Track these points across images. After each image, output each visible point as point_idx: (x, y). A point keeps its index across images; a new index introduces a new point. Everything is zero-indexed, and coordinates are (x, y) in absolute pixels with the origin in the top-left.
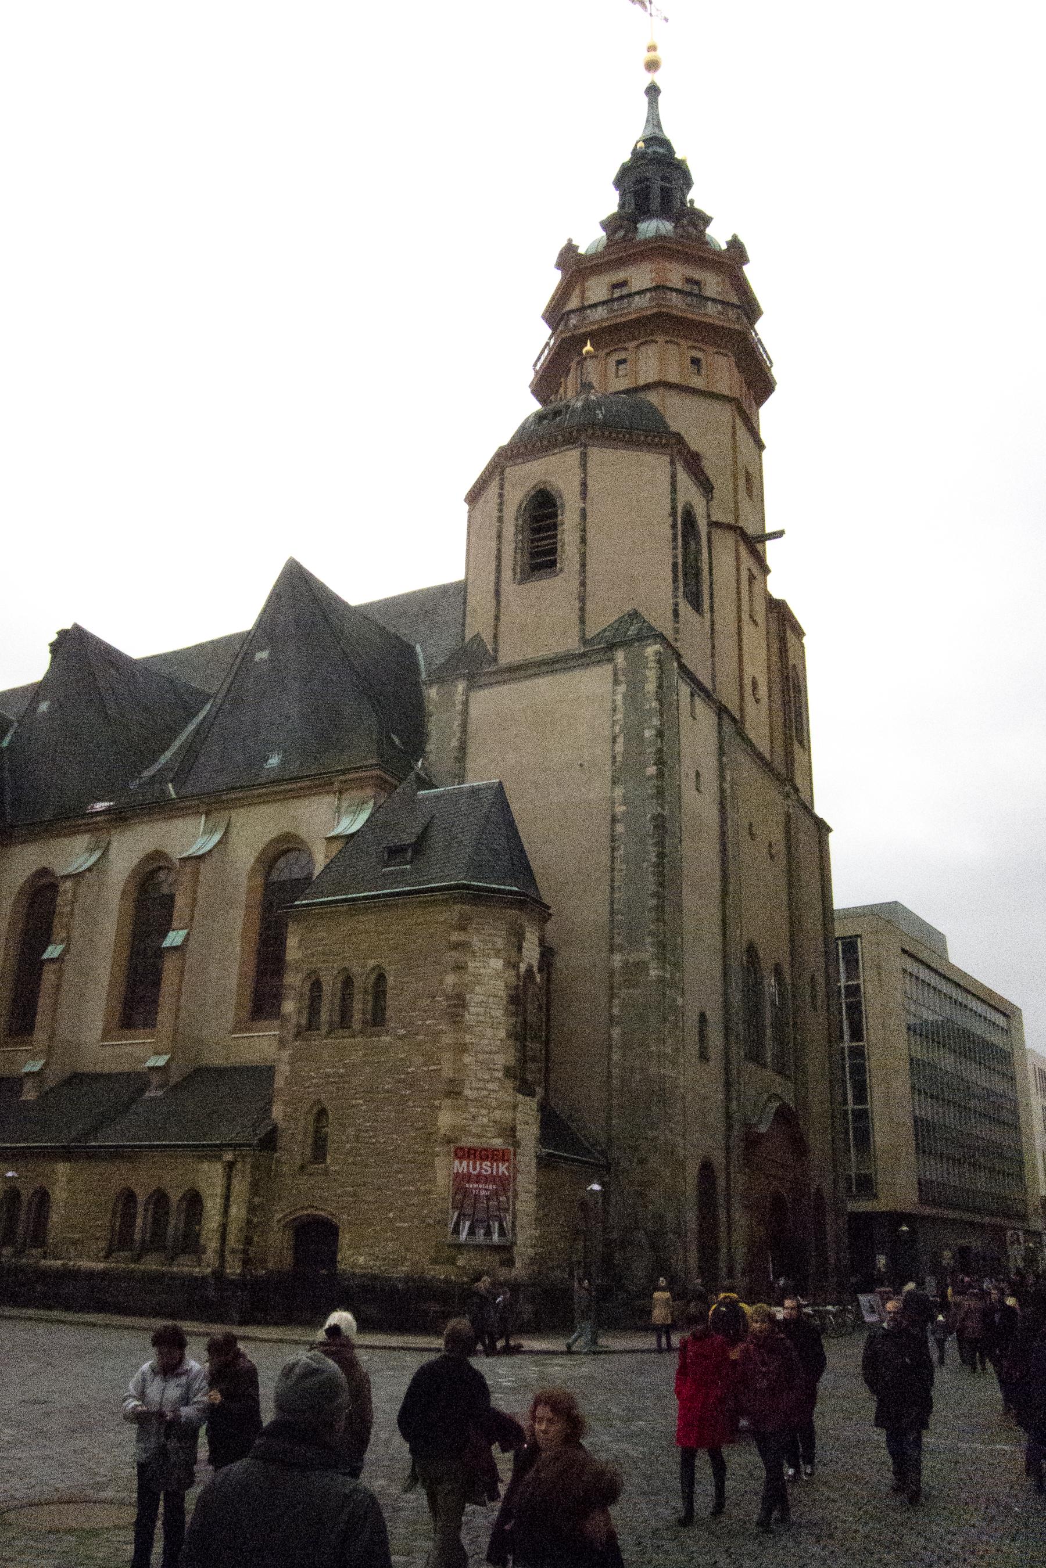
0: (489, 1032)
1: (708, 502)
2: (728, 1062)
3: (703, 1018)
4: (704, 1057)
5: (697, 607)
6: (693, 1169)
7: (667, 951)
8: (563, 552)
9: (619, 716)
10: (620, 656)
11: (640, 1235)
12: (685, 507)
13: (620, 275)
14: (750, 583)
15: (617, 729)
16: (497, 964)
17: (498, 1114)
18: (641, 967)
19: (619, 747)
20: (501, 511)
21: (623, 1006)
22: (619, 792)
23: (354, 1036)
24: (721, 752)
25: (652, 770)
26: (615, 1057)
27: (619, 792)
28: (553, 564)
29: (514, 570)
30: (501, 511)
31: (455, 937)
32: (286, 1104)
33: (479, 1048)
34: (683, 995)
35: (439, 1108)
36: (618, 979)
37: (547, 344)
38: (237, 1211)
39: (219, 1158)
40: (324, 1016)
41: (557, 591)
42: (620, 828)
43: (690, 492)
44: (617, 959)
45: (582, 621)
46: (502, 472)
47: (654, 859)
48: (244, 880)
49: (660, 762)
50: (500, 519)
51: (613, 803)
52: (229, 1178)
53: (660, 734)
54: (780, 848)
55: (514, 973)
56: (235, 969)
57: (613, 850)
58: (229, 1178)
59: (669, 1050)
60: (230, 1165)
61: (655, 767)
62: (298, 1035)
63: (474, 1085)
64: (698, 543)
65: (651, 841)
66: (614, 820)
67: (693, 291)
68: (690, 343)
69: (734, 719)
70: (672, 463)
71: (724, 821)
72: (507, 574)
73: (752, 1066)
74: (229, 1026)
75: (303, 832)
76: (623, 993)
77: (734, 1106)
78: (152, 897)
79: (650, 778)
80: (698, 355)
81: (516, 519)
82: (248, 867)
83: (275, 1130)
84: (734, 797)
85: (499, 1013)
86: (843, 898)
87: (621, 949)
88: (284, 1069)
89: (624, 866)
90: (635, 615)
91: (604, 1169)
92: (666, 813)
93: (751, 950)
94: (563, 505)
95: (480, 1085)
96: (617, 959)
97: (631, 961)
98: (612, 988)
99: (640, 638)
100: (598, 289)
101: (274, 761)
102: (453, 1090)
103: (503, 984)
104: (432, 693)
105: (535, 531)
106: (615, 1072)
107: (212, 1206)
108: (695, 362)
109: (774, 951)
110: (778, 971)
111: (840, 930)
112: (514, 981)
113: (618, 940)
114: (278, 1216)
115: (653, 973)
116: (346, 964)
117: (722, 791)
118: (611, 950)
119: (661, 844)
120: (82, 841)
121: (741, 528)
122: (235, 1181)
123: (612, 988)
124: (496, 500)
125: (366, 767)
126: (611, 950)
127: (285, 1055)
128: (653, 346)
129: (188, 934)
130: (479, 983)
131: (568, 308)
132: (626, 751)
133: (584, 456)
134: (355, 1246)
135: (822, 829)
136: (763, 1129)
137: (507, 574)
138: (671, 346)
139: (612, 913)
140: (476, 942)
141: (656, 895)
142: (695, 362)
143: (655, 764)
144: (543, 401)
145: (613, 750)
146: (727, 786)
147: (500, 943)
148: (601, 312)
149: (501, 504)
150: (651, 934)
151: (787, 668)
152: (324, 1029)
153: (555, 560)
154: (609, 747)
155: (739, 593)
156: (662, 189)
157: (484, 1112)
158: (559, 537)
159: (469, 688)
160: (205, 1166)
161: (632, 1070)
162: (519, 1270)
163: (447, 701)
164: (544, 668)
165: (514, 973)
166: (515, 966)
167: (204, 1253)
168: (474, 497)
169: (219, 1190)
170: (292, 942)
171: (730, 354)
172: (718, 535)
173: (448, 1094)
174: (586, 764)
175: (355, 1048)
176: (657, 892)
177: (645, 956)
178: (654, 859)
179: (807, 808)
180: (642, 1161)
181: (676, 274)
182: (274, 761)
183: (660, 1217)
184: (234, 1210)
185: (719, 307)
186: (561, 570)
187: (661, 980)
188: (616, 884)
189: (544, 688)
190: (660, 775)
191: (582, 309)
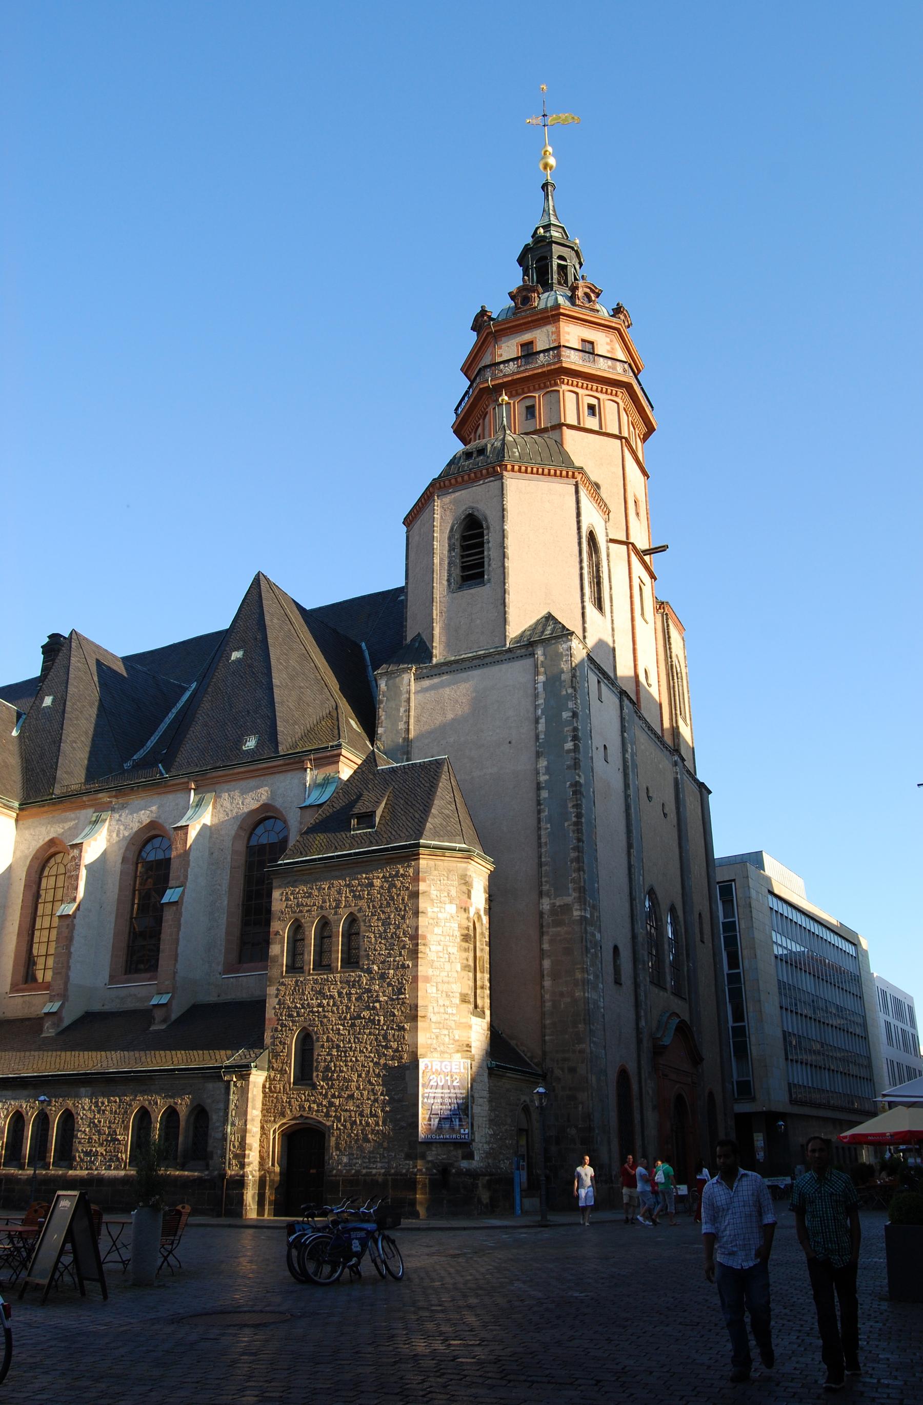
0: (447, 966)
2: (636, 985)
3: (616, 949)
4: (618, 982)
5: (600, 607)
6: (613, 1075)
7: (586, 894)
8: (489, 565)
9: (541, 701)
10: (539, 652)
11: (573, 1131)
13: (526, 337)
15: (539, 712)
16: (452, 909)
17: (457, 1034)
18: (567, 908)
19: (542, 727)
21: (551, 942)
22: (543, 763)
24: (623, 729)
25: (569, 745)
26: (547, 983)
27: (543, 763)
28: (482, 575)
29: (448, 580)
33: (439, 980)
34: (600, 932)
36: (547, 919)
37: (467, 393)
42: (544, 794)
43: (592, 517)
47: (574, 819)
49: (575, 738)
53: (575, 715)
54: (671, 808)
55: (465, 915)
56: (223, 920)
57: (539, 812)
59: (591, 977)
61: (572, 743)
63: (436, 1010)
64: (598, 557)
65: (570, 805)
66: (539, 787)
69: (630, 700)
70: (577, 492)
71: (626, 786)
73: (656, 990)
74: (220, 968)
76: (552, 930)
77: (643, 1023)
79: (569, 751)
84: (635, 766)
85: (453, 950)
86: (721, 850)
87: (549, 896)
89: (549, 826)
90: (549, 617)
91: (543, 1077)
92: (582, 781)
93: (651, 893)
94: (488, 528)
97: (558, 904)
98: (542, 926)
100: (508, 349)
101: (251, 743)
103: (457, 925)
104: (383, 685)
105: (464, 548)
106: (547, 997)
109: (669, 892)
110: (673, 909)
111: (721, 875)
112: (465, 923)
113: (545, 888)
115: (576, 913)
116: (324, 913)
117: (625, 761)
119: (577, 806)
121: (633, 544)
123: (542, 926)
126: (541, 894)
130: (437, 924)
131: (482, 364)
135: (704, 790)
136: (667, 1041)
139: (540, 865)
140: (434, 893)
141: (577, 849)
142: (591, 408)
143: (572, 740)
144: (465, 441)
145: (536, 728)
146: (628, 756)
147: (453, 893)
148: (512, 366)
153: (483, 572)
154: (533, 727)
155: (631, 597)
156: (559, 265)
157: (446, 1032)
158: (486, 553)
160: (210, 1085)
161: (562, 994)
162: (477, 1163)
164: (476, 662)
165: (465, 915)
166: (466, 910)
167: (212, 1158)
168: (409, 521)
170: (276, 894)
174: (513, 742)
176: (578, 847)
177: (568, 900)
178: (574, 819)
179: (692, 775)
180: (572, 1070)
182: (251, 743)
186: (489, 580)
187: (583, 918)
188: (543, 840)
190: (576, 749)
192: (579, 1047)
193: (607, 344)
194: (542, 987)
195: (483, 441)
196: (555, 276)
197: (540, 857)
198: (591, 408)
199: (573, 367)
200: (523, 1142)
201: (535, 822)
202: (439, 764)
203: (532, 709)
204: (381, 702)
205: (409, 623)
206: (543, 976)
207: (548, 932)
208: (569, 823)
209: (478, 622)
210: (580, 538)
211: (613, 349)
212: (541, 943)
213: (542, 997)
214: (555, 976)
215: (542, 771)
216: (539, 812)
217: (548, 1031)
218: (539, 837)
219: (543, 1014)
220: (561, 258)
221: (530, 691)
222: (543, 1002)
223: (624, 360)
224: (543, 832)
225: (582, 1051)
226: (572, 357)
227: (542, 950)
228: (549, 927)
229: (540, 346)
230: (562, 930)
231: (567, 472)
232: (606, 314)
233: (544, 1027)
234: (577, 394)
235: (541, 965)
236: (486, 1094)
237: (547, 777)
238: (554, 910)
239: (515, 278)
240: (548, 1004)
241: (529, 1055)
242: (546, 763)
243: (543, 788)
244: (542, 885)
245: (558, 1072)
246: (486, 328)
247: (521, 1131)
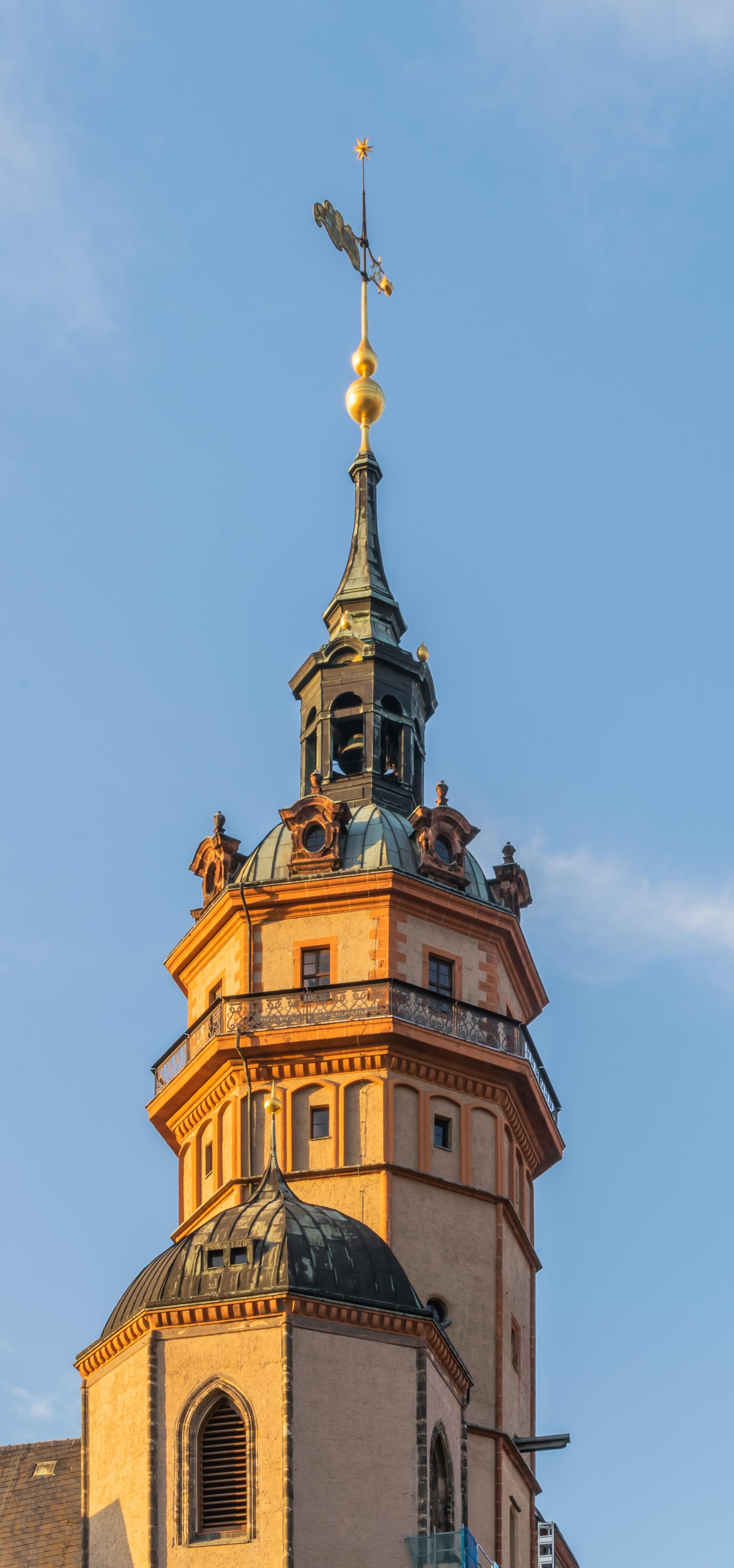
1: (463, 1408)
12: (435, 1429)
14: (512, 1518)
64: (449, 1487)
68: (436, 1089)
80: (446, 1110)
121: (505, 1436)
158: (248, 1478)
193: (482, 967)
198: (442, 1123)
210: (423, 1460)
211: (490, 979)
231: (404, 1322)
234: (416, 1091)
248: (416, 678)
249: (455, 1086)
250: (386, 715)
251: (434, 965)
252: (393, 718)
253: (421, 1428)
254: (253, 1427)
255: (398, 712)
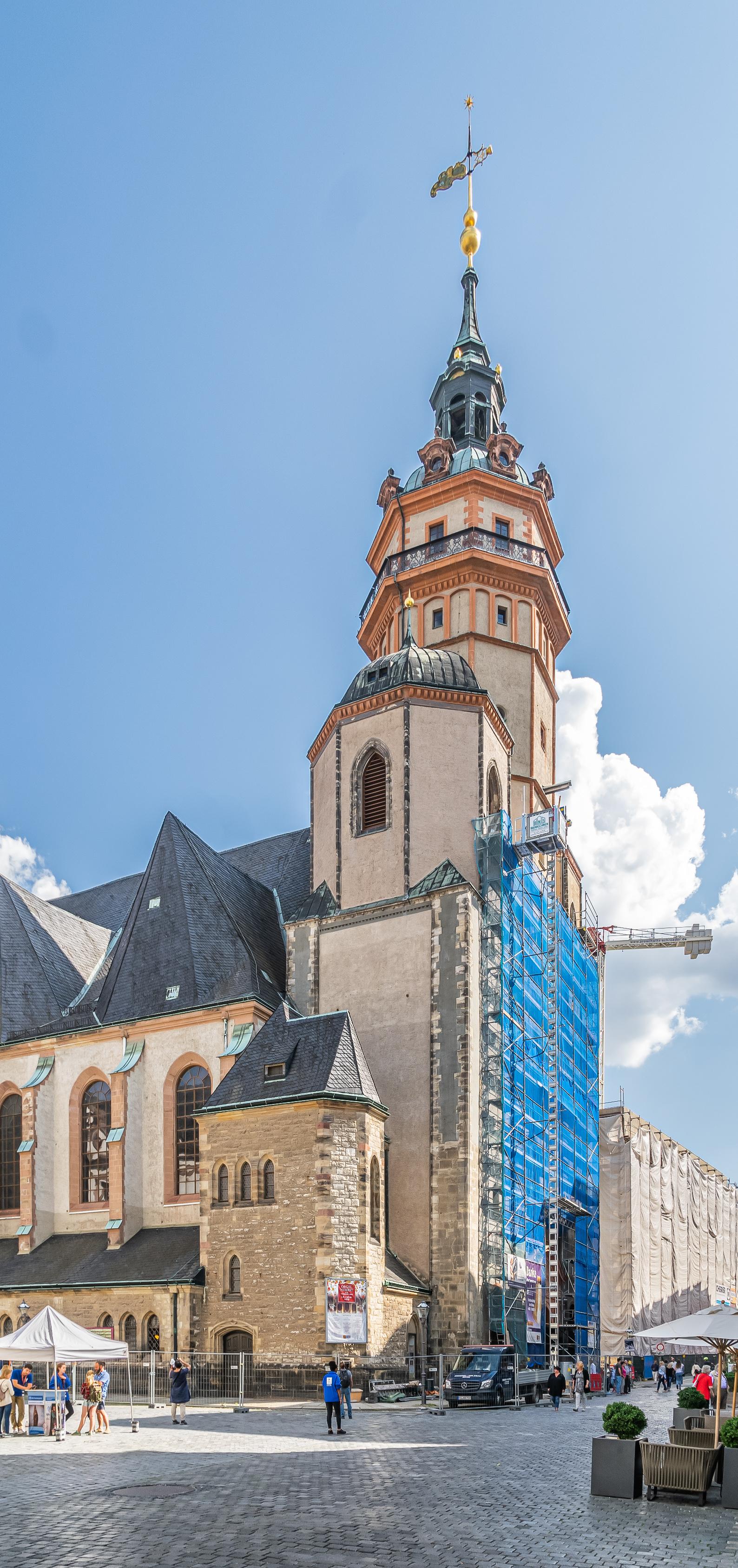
11: (452, 1336)
15: (435, 966)
18: (453, 1151)
19: (436, 981)
20: (338, 768)
21: (439, 1181)
22: (436, 1017)
23: (252, 1205)
26: (435, 1216)
29: (351, 824)
30: (338, 768)
31: (321, 1133)
32: (208, 1253)
35: (316, 1254)
36: (436, 1161)
38: (184, 1325)
39: (167, 1291)
40: (231, 1192)
41: (386, 840)
42: (437, 1046)
43: (495, 752)
44: (435, 1148)
45: (407, 871)
46: (338, 732)
47: (462, 1071)
48: (160, 1090)
50: (339, 777)
51: (432, 1026)
52: (175, 1303)
57: (432, 1063)
58: (175, 1303)
60: (176, 1296)
62: (213, 1206)
64: (499, 798)
66: (432, 1040)
67: (502, 535)
72: (346, 828)
75: (201, 1052)
76: (441, 1170)
78: (95, 1105)
81: (352, 776)
82: (164, 1079)
83: (203, 1269)
87: (438, 1140)
88: (205, 1231)
89: (440, 1076)
95: (344, 1238)
96: (435, 1148)
98: (431, 1167)
99: (452, 885)
102: (324, 1242)
106: (434, 1227)
107: (165, 1324)
108: (502, 611)
113: (436, 1133)
114: (210, 1329)
115: (461, 1156)
118: (431, 1139)
120: (33, 1060)
122: (178, 1306)
123: (431, 1167)
124: (334, 758)
125: (246, 999)
126: (431, 1139)
127: (205, 1219)
128: (464, 597)
129: (124, 1133)
131: (389, 553)
132: (440, 987)
133: (407, 716)
134: (265, 1346)
137: (346, 828)
138: (482, 595)
139: (432, 1112)
145: (432, 982)
149: (338, 762)
150: (460, 1127)
151: (566, 906)
152: (232, 1201)
154: (429, 980)
156: (477, 408)
158: (387, 794)
159: (320, 931)
160: (158, 1297)
161: (447, 1226)
163: (302, 937)
169: (169, 1312)
171: (531, 601)
172: (515, 784)
173: (321, 1245)
175: (257, 1213)
177: (454, 1144)
178: (462, 1071)
180: (454, 1288)
181: (488, 512)
183: (465, 1325)
184: (180, 1325)
185: (525, 550)
188: (435, 1090)
189: (377, 930)
191: (403, 553)
192: (459, 1269)
194: (431, 1219)
195: (387, 658)
196: (472, 425)
197: (432, 1105)
199: (485, 558)
200: (412, 1343)
201: (429, 1072)
202: (342, 1017)
203: (428, 962)
204: (290, 953)
205: (315, 870)
206: (431, 1210)
207: (436, 1172)
208: (458, 1074)
209: (380, 870)
212: (431, 1181)
213: (430, 1226)
214: (442, 1210)
215: (436, 1024)
216: (432, 1063)
217: (434, 1256)
218: (432, 1087)
219: (431, 1241)
220: (480, 396)
221: (428, 945)
222: (431, 1231)
223: (541, 546)
224: (435, 1082)
225: (461, 1273)
226: (485, 543)
227: (431, 1188)
228: (437, 1168)
229: (449, 530)
230: (448, 1170)
232: (526, 483)
233: (431, 1252)
235: (430, 1200)
236: (381, 1306)
237: (439, 1030)
238: (442, 1154)
239: (426, 428)
240: (435, 1234)
241: (419, 1274)
242: (439, 1017)
243: (436, 1041)
244: (432, 1131)
245: (442, 1289)
246: (395, 500)
247: (410, 1335)
248: (493, 382)
249: (509, 589)
250: (477, 403)
251: (499, 526)
252: (481, 404)
253: (481, 765)
254: (389, 765)
255: (484, 401)
